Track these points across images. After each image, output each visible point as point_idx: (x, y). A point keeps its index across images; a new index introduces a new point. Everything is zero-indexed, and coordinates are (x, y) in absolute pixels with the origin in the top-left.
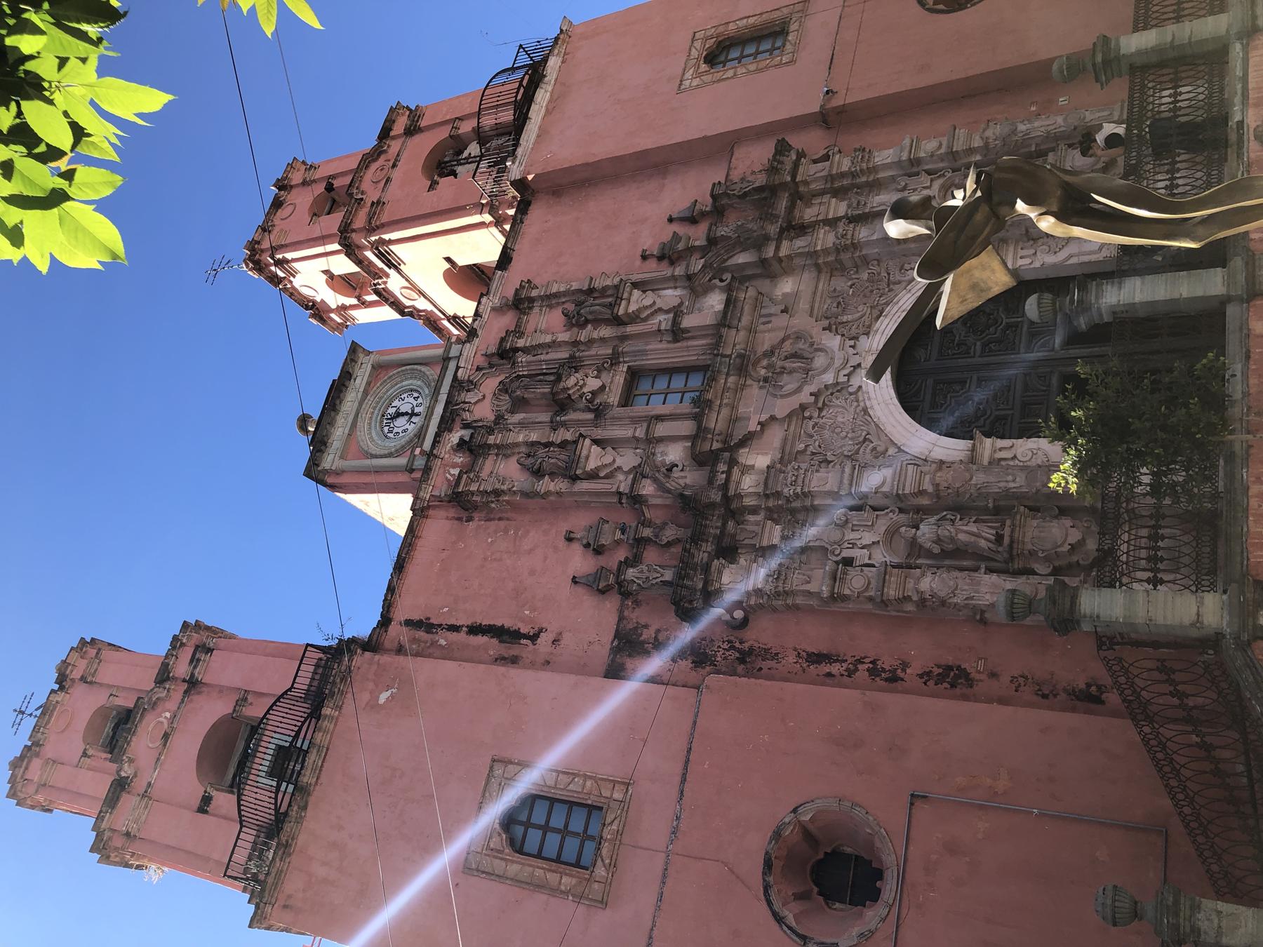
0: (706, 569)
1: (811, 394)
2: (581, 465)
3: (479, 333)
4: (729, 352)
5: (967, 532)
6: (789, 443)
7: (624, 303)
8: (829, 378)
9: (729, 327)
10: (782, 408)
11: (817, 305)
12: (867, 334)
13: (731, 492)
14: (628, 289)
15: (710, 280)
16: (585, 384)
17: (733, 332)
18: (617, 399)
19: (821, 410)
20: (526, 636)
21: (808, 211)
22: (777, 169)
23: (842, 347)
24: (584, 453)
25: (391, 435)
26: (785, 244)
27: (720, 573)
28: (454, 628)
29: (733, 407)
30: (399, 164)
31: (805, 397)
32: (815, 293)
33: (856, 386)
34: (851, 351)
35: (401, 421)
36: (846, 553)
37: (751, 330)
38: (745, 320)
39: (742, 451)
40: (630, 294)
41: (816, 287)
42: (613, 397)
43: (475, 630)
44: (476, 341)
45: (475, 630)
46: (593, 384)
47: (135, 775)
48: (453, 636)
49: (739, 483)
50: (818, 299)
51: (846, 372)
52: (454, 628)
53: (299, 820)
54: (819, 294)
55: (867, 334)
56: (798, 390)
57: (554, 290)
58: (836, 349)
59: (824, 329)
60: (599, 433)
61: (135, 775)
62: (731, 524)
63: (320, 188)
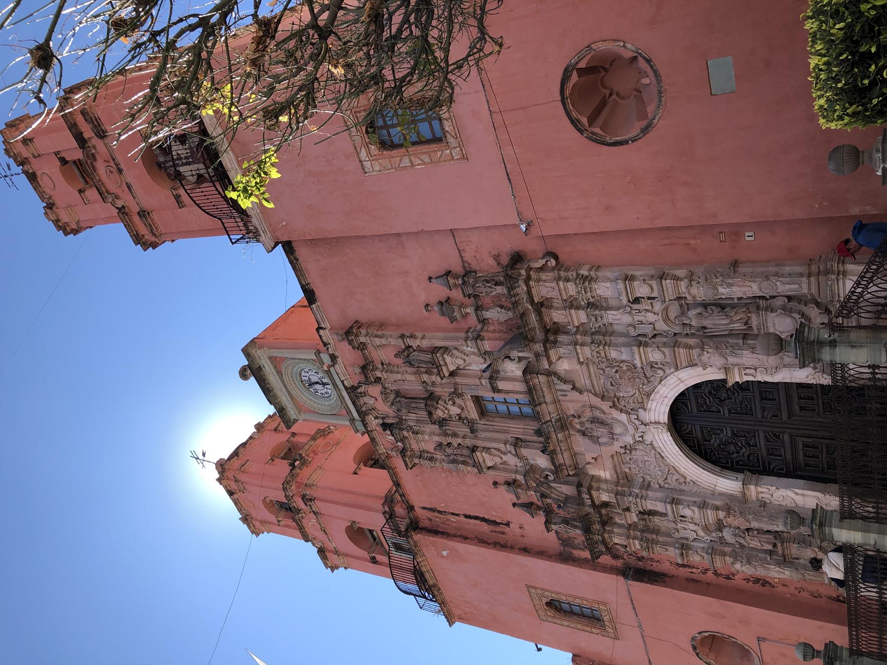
0: (604, 542)
3: (336, 354)
8: (629, 440)
9: (540, 404)
11: (595, 382)
13: (597, 503)
14: (440, 359)
17: (544, 406)
22: (516, 302)
23: (630, 421)
24: (481, 460)
28: (457, 515)
29: (569, 449)
30: (122, 166)
34: (637, 422)
37: (556, 401)
38: (548, 398)
40: (444, 359)
43: (467, 516)
44: (339, 360)
45: (467, 516)
46: (455, 410)
50: (594, 378)
52: (457, 515)
53: (441, 594)
54: (593, 374)
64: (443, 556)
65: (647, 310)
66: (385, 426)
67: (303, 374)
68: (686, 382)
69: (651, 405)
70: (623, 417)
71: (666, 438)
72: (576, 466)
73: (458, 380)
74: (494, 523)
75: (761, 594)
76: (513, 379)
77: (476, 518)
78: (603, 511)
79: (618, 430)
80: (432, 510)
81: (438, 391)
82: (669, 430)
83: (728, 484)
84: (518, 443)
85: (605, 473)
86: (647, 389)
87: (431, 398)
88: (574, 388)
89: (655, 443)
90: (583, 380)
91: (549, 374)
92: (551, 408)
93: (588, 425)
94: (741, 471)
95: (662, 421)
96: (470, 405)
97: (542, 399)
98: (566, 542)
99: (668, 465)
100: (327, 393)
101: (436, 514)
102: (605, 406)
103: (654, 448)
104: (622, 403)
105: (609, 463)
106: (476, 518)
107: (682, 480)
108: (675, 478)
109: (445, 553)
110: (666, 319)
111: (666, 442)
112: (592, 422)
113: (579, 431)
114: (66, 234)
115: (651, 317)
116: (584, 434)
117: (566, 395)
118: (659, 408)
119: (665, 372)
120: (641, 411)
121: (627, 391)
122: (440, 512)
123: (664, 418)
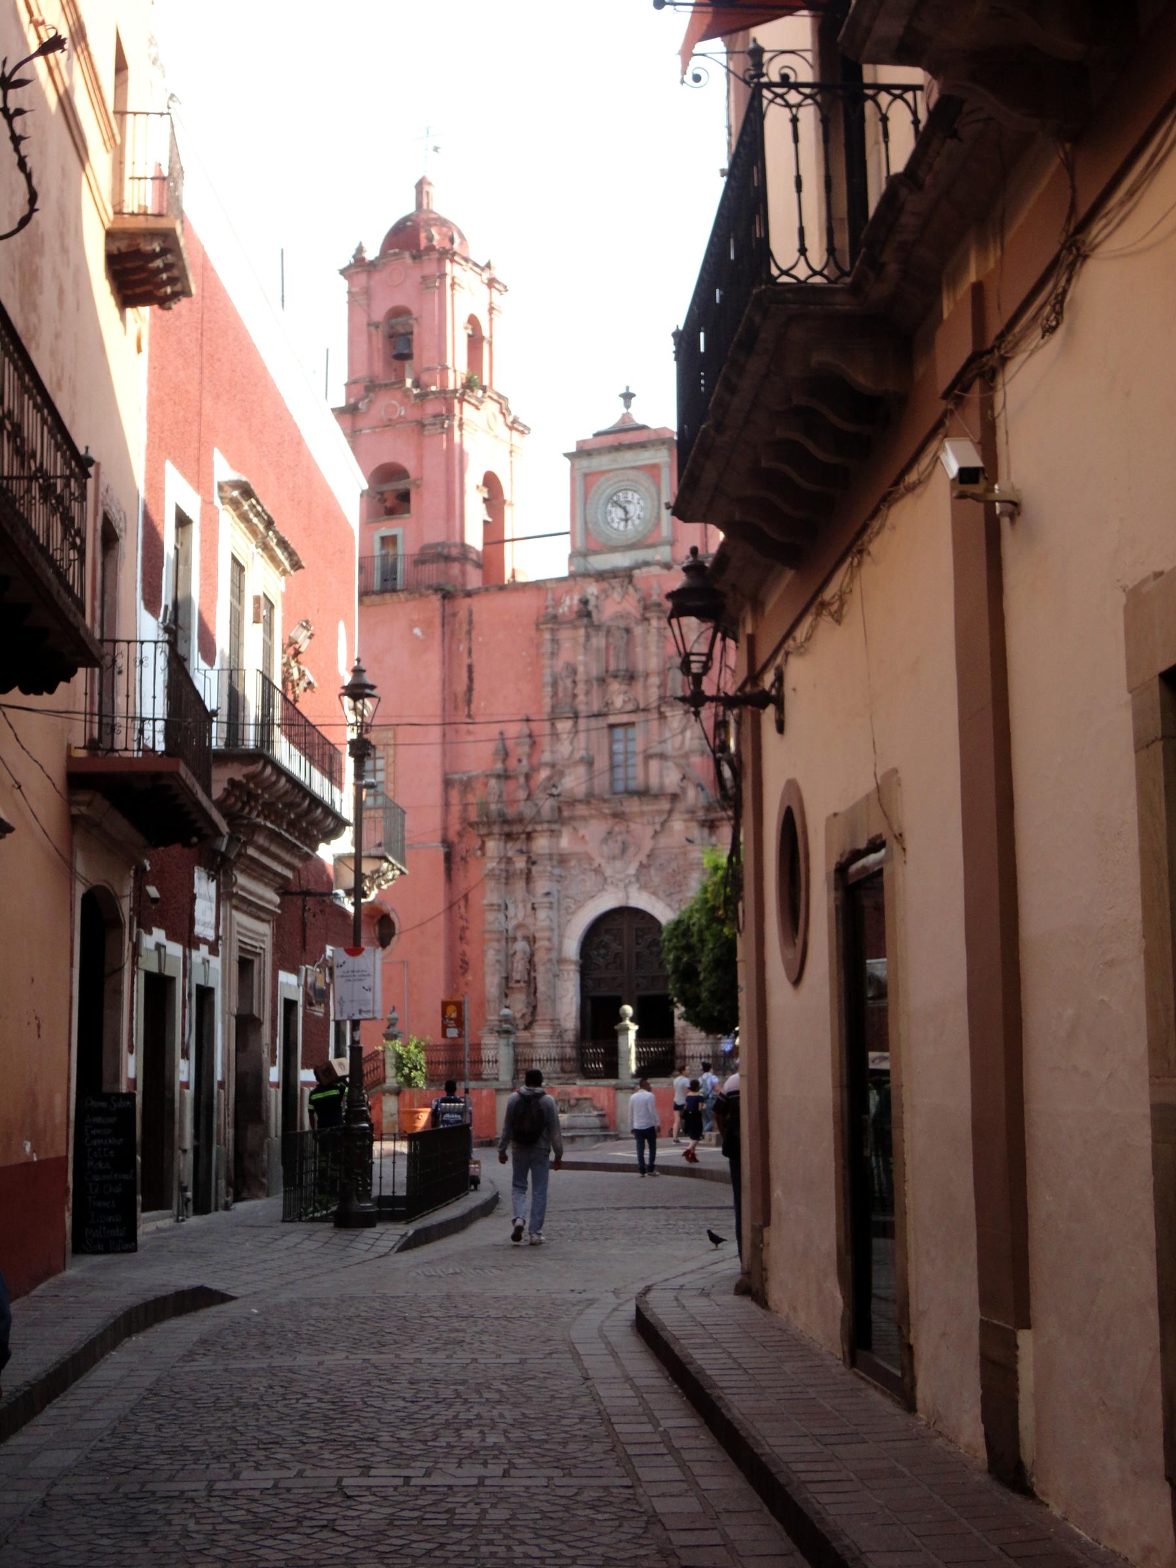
5: (519, 967)
8: (608, 872)
10: (592, 847)
20: (469, 711)
23: (628, 876)
29: (591, 817)
31: (598, 861)
35: (620, 513)
37: (642, 813)
38: (646, 808)
42: (612, 719)
43: (470, 668)
44: (665, 572)
45: (470, 668)
46: (618, 702)
48: (466, 655)
56: (602, 856)
64: (411, 628)
66: (585, 602)
67: (636, 496)
70: (632, 870)
72: (572, 818)
74: (469, 702)
75: (459, 966)
76: (661, 776)
77: (471, 679)
78: (523, 836)
79: (618, 864)
80: (470, 622)
81: (639, 685)
83: (572, 948)
84: (589, 763)
85: (565, 842)
86: (661, 893)
87: (630, 677)
88: (656, 832)
89: (604, 893)
90: (663, 841)
91: (670, 812)
93: (619, 838)
94: (581, 957)
98: (466, 786)
100: (613, 520)
101: (465, 627)
102: (642, 857)
105: (578, 848)
106: (471, 679)
109: (417, 631)
111: (607, 902)
112: (623, 843)
116: (610, 833)
120: (637, 886)
121: (655, 876)
122: (469, 632)
123: (633, 903)
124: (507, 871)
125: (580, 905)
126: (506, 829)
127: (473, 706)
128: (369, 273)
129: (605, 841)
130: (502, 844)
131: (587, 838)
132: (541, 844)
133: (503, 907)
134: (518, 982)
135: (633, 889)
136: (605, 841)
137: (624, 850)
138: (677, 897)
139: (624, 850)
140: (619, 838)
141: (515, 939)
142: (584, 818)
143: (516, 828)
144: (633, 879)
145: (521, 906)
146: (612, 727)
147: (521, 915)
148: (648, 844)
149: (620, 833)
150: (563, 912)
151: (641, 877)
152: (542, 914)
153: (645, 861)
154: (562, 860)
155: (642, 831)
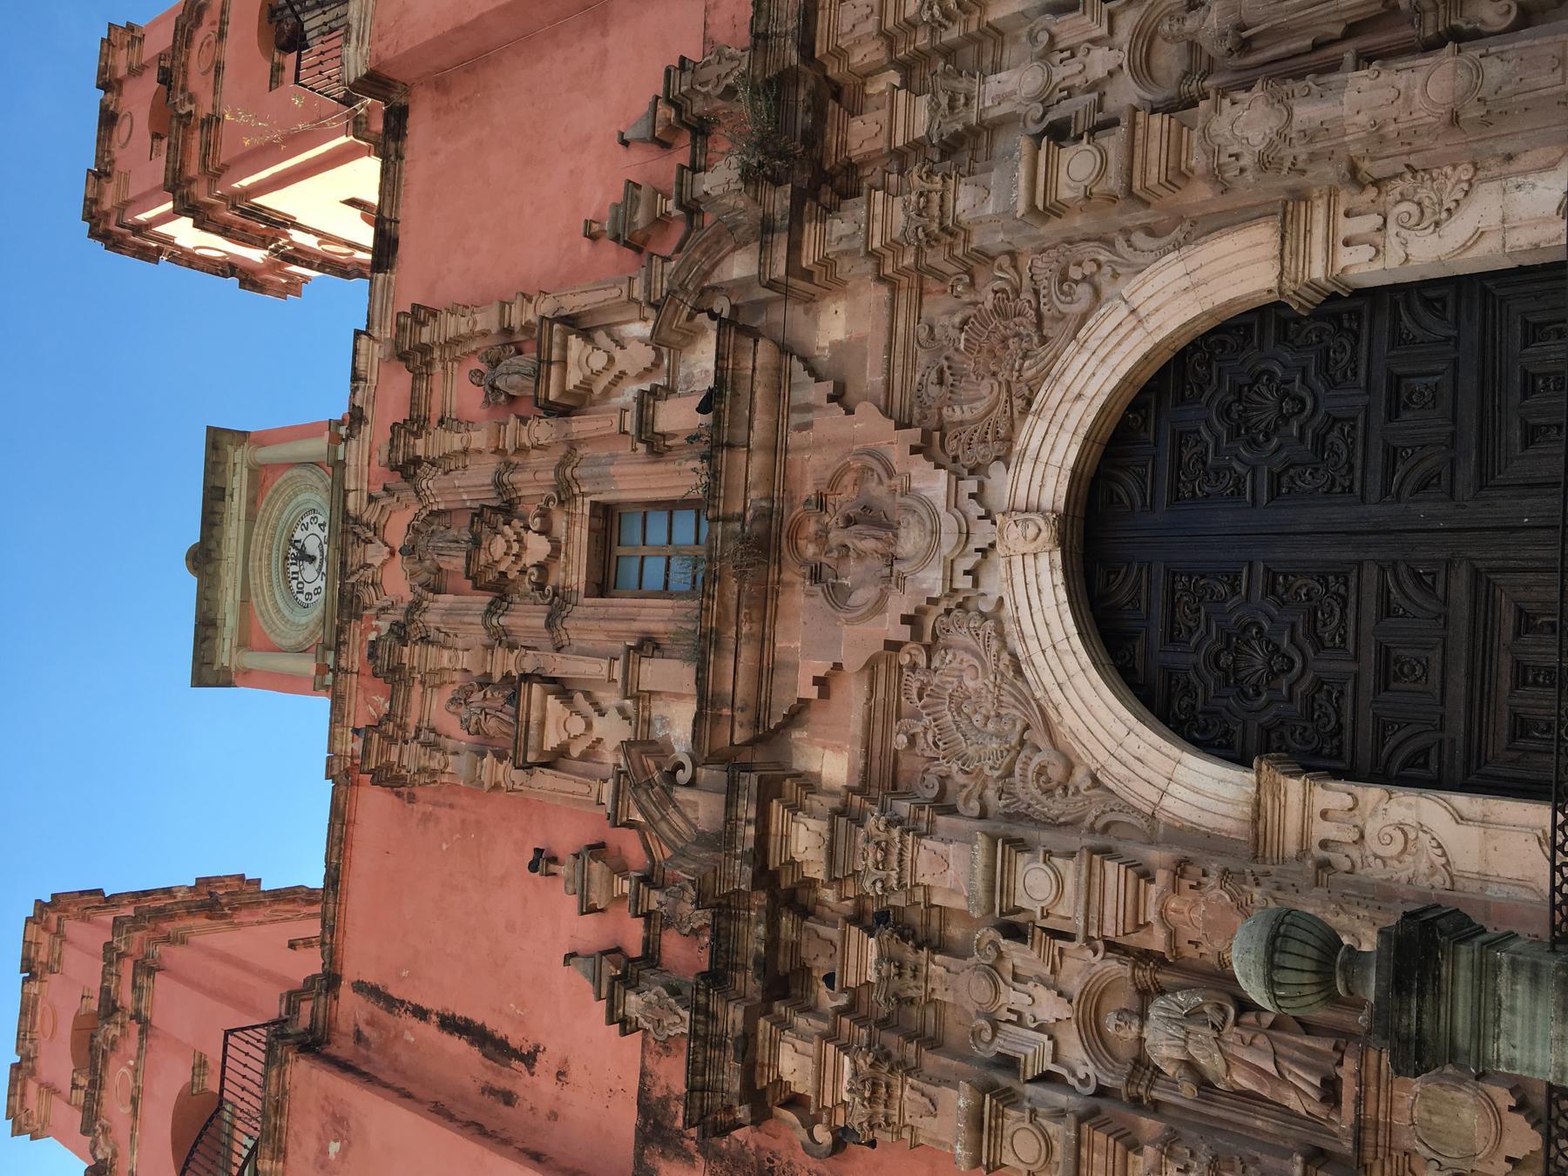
0: (747, 1042)
1: (906, 619)
2: (532, 742)
3: (368, 413)
4: (739, 509)
6: (878, 727)
7: (554, 370)
8: (932, 580)
9: (730, 446)
11: (898, 375)
12: (1004, 459)
13: (774, 862)
14: (556, 339)
15: (690, 318)
16: (523, 547)
18: (583, 577)
19: (929, 650)
21: (856, 124)
23: (953, 502)
24: (535, 715)
25: (301, 597)
26: (810, 232)
27: (774, 1045)
28: (421, 1013)
29: (764, 641)
30: (229, 29)
32: (890, 347)
33: (993, 598)
34: (975, 510)
36: (1001, 1045)
37: (777, 448)
38: (759, 433)
39: (797, 734)
40: (565, 347)
41: (892, 331)
42: (574, 573)
43: (451, 1024)
44: (366, 430)
45: (451, 1024)
46: (538, 547)
47: (115, 1155)
49: (785, 837)
51: (968, 563)
52: (421, 1013)
54: (899, 347)
55: (1004, 459)
56: (879, 607)
57: (451, 333)
58: (940, 504)
59: (915, 450)
60: (561, 666)
61: (115, 1155)
62: (786, 922)
63: (152, 76)
65: (1094, 42)
68: (1151, 324)
69: (1031, 434)
71: (1046, 579)
73: (579, 426)
79: (910, 541)
82: (1062, 541)
88: (837, 397)
91: (785, 349)
92: (758, 461)
95: (1047, 504)
96: (579, 537)
97: (741, 433)
99: (1024, 700)
103: (1001, 635)
104: (951, 445)
107: (1056, 772)
108: (1037, 759)
110: (1143, 69)
112: (849, 521)
113: (805, 563)
114: (93, 234)
115: (1100, 62)
116: (816, 575)
117: (807, 426)
118: (1047, 459)
119: (1097, 292)
120: (996, 470)
121: (974, 404)
123: (1053, 490)
124: (884, 1024)
125: (1040, 722)
126: (750, 983)
127: (514, 1042)
128: (33, 1073)
129: (837, 595)
130: (801, 1021)
131: (821, 667)
132: (804, 841)
133: (1004, 1080)
134: (1330, 1091)
135: (1004, 485)
136: (837, 595)
137: (869, 517)
138: (1054, 303)
139: (869, 517)
140: (836, 537)
141: (1141, 1064)
142: (766, 671)
143: (754, 937)
144: (970, 485)
145: (1013, 997)
146: (602, 584)
147: (1049, 1008)
148: (868, 425)
149: (822, 536)
150: (1056, 807)
151: (969, 453)
152: (1035, 885)
153: (914, 435)
154: (881, 778)
155: (828, 443)
